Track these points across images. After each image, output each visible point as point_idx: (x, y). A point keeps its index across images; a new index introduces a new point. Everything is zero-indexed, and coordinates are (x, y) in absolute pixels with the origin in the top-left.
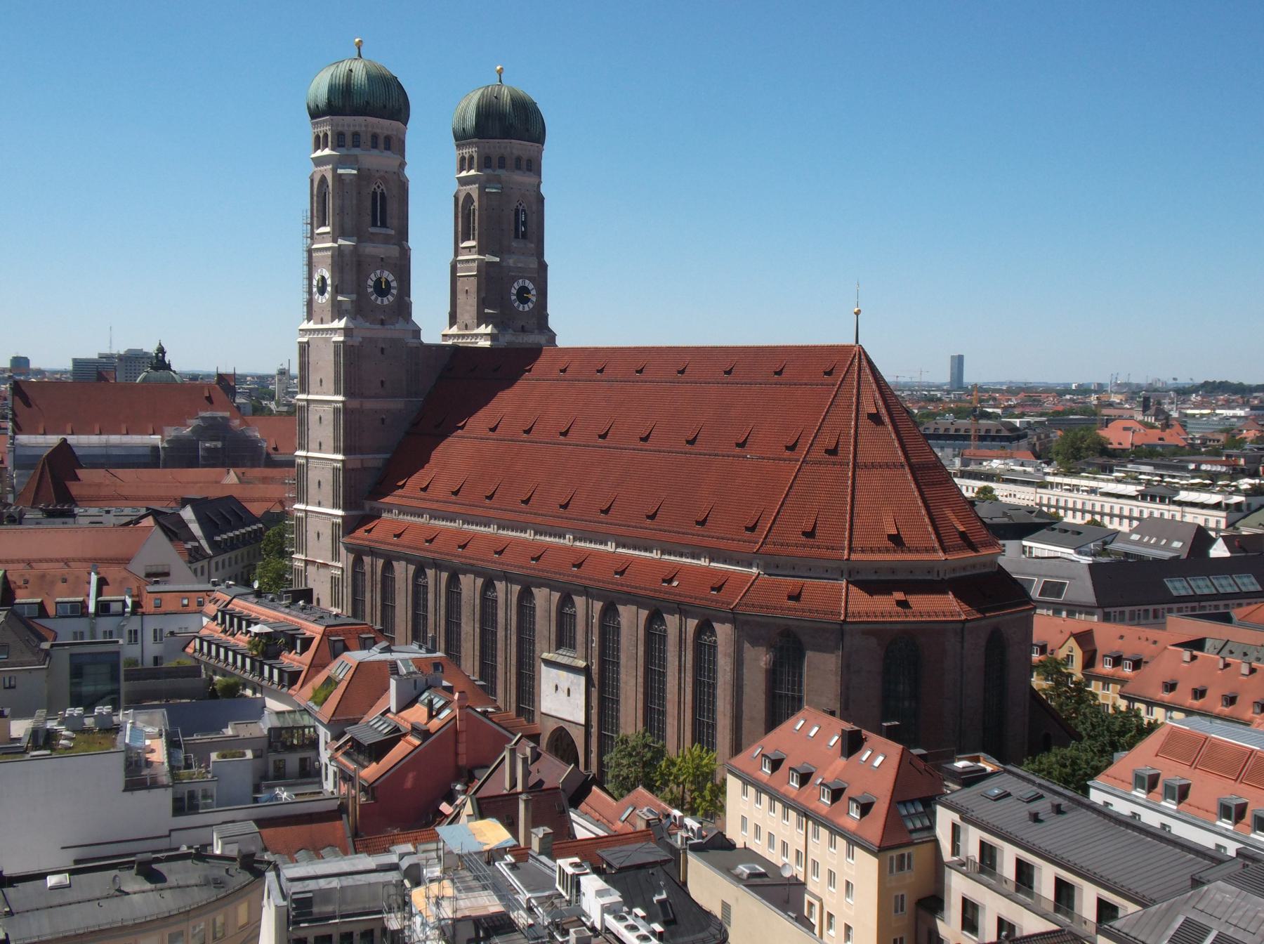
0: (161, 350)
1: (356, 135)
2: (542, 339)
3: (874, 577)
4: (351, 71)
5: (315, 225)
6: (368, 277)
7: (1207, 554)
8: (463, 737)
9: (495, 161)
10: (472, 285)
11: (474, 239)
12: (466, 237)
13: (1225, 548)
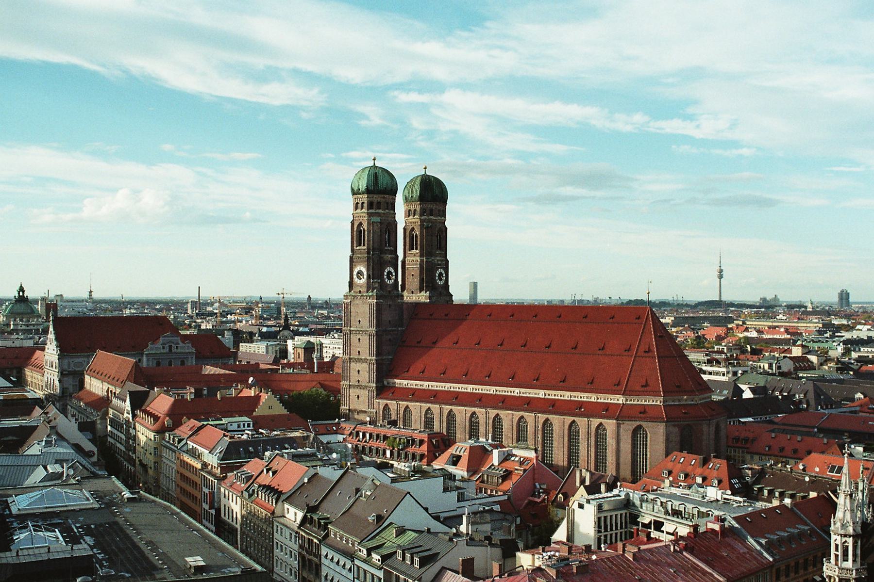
0: (22, 289)
1: (379, 203)
2: (448, 298)
3: (673, 403)
4: (376, 173)
5: (355, 245)
6: (384, 271)
7: (742, 396)
8: (536, 472)
9: (428, 212)
10: (417, 272)
11: (416, 249)
12: (412, 248)
13: (751, 393)
